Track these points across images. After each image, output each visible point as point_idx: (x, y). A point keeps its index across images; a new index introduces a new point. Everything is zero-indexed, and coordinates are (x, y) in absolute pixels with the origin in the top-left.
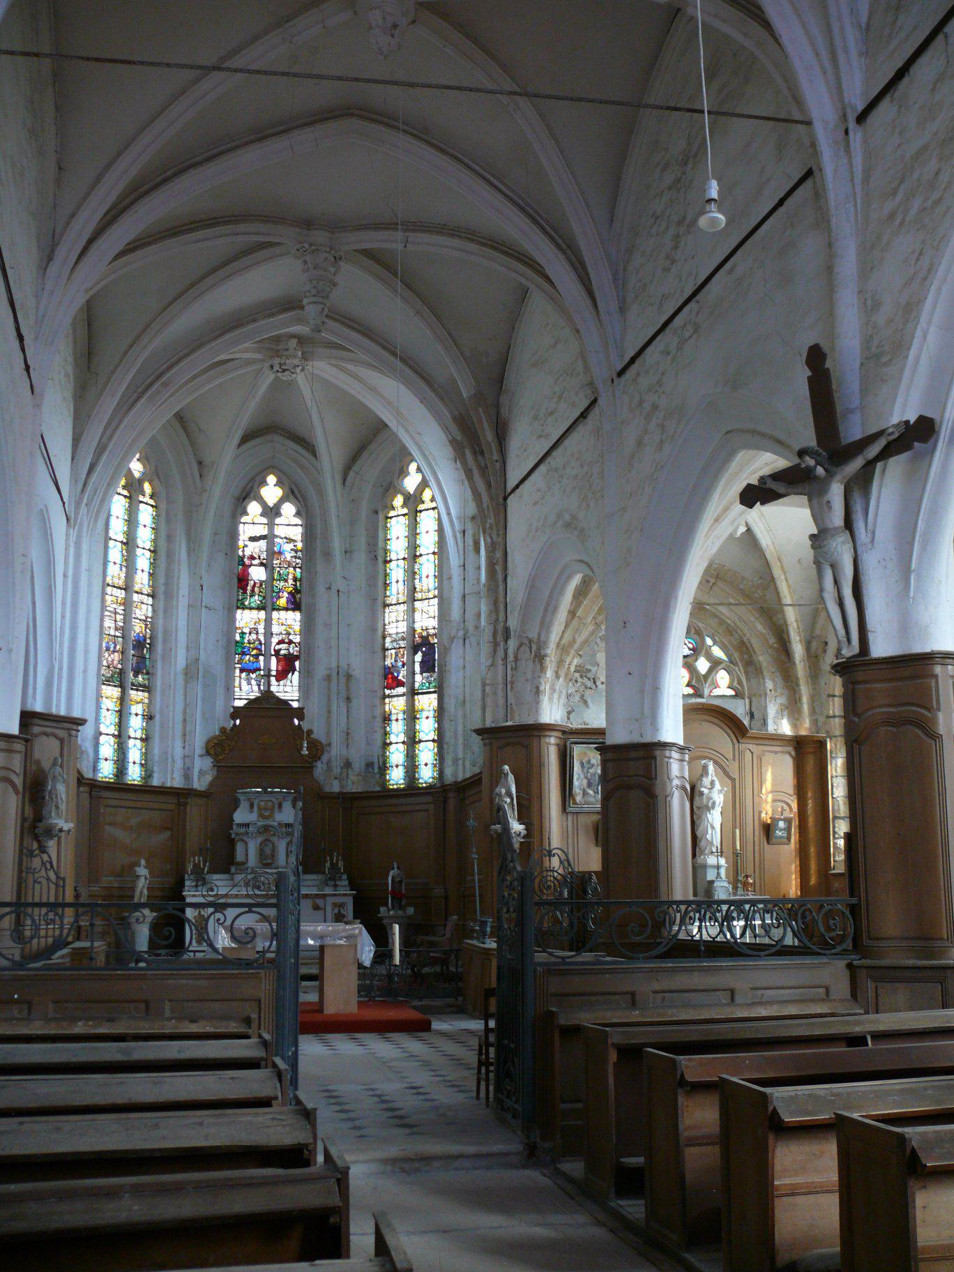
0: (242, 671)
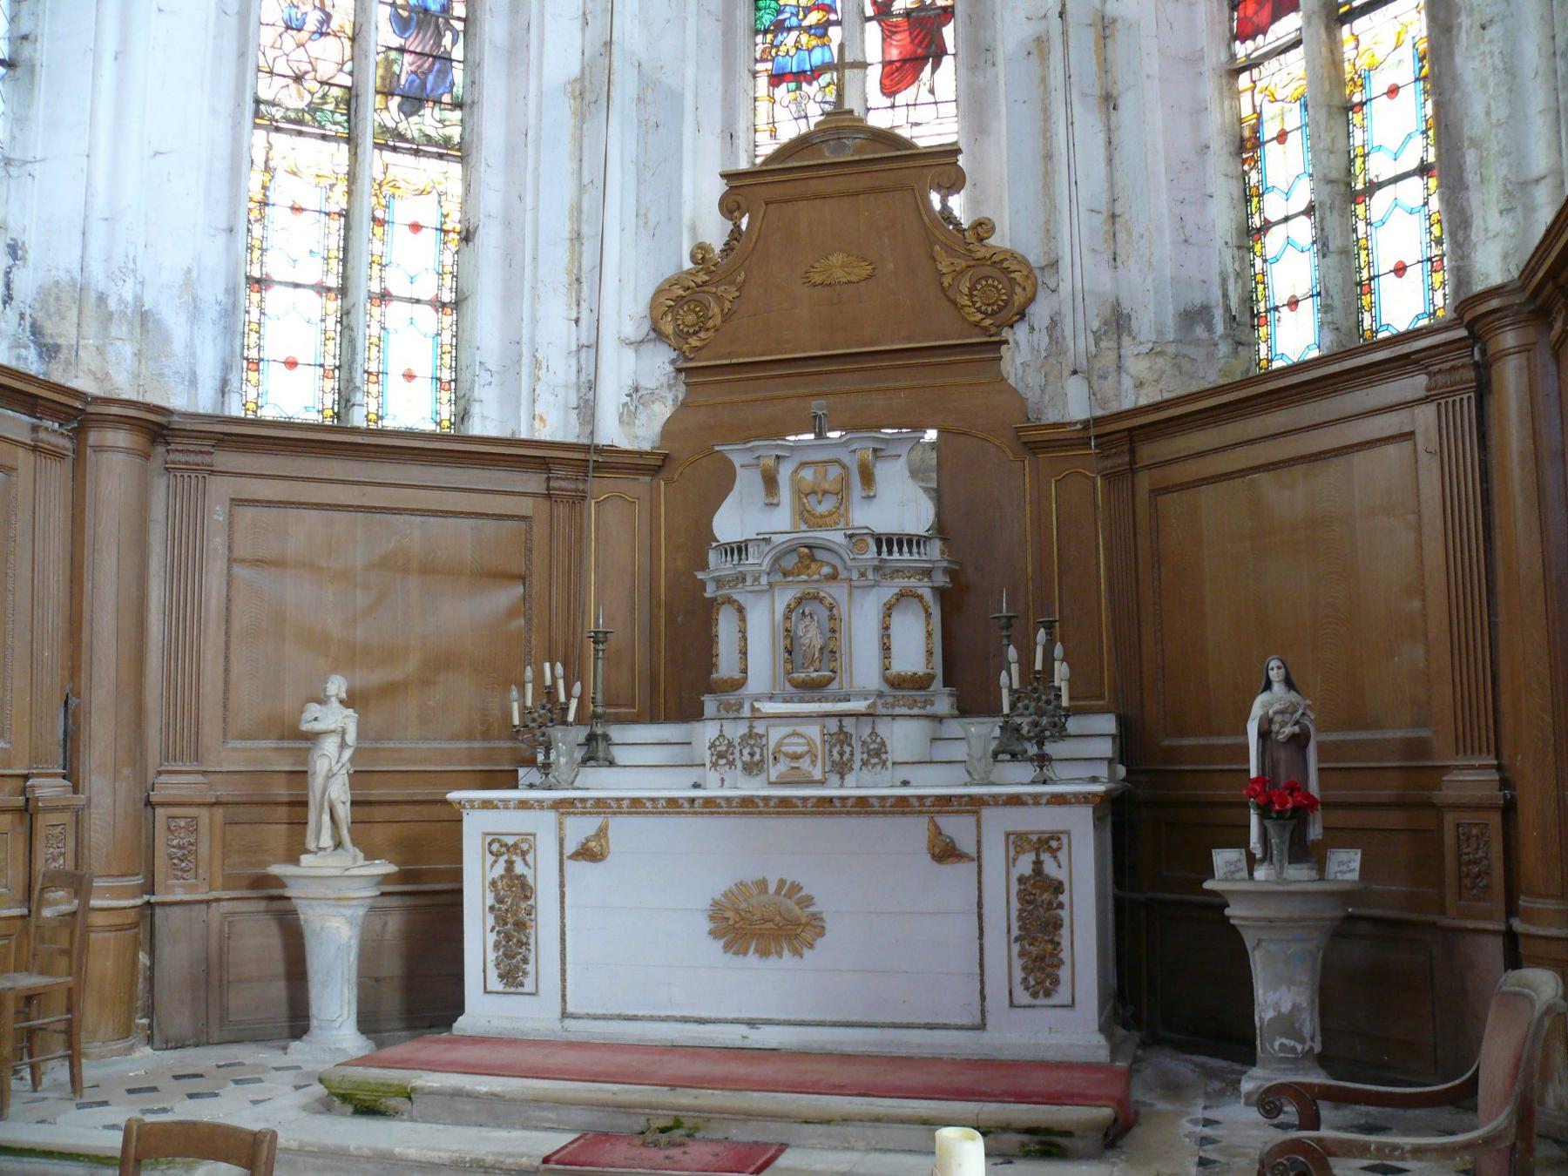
0: (776, 79)
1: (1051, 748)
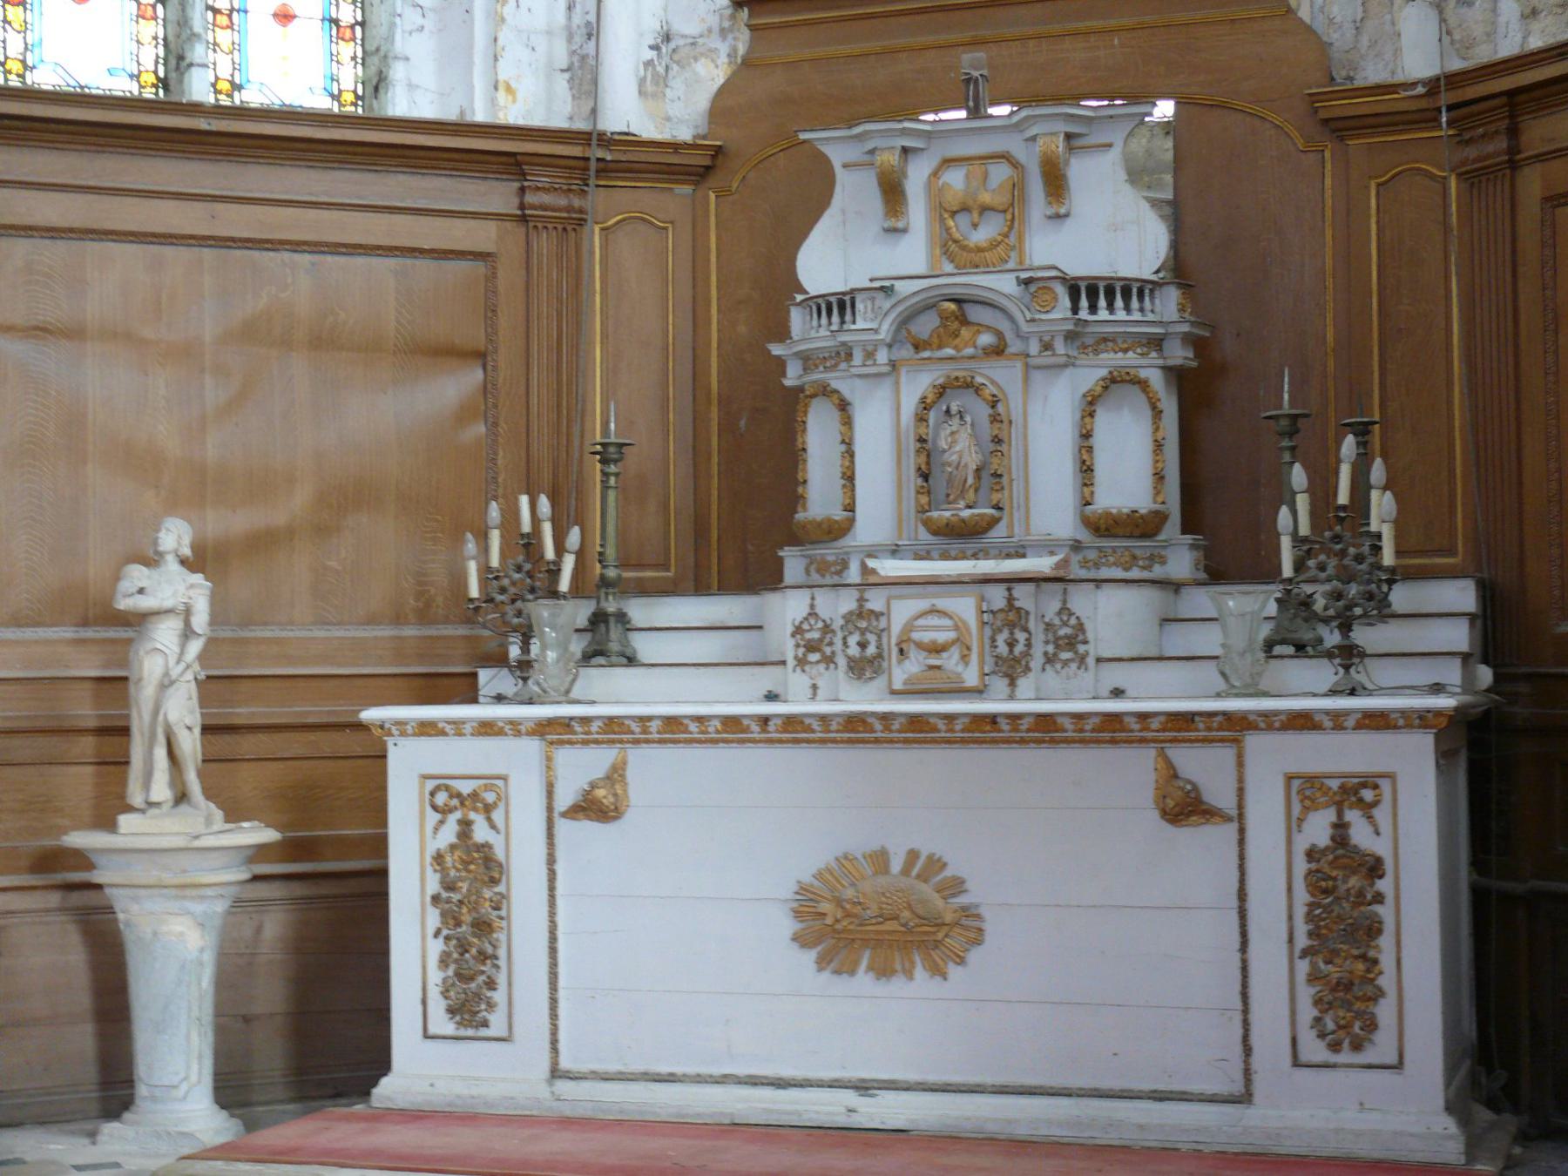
1: (1363, 636)
